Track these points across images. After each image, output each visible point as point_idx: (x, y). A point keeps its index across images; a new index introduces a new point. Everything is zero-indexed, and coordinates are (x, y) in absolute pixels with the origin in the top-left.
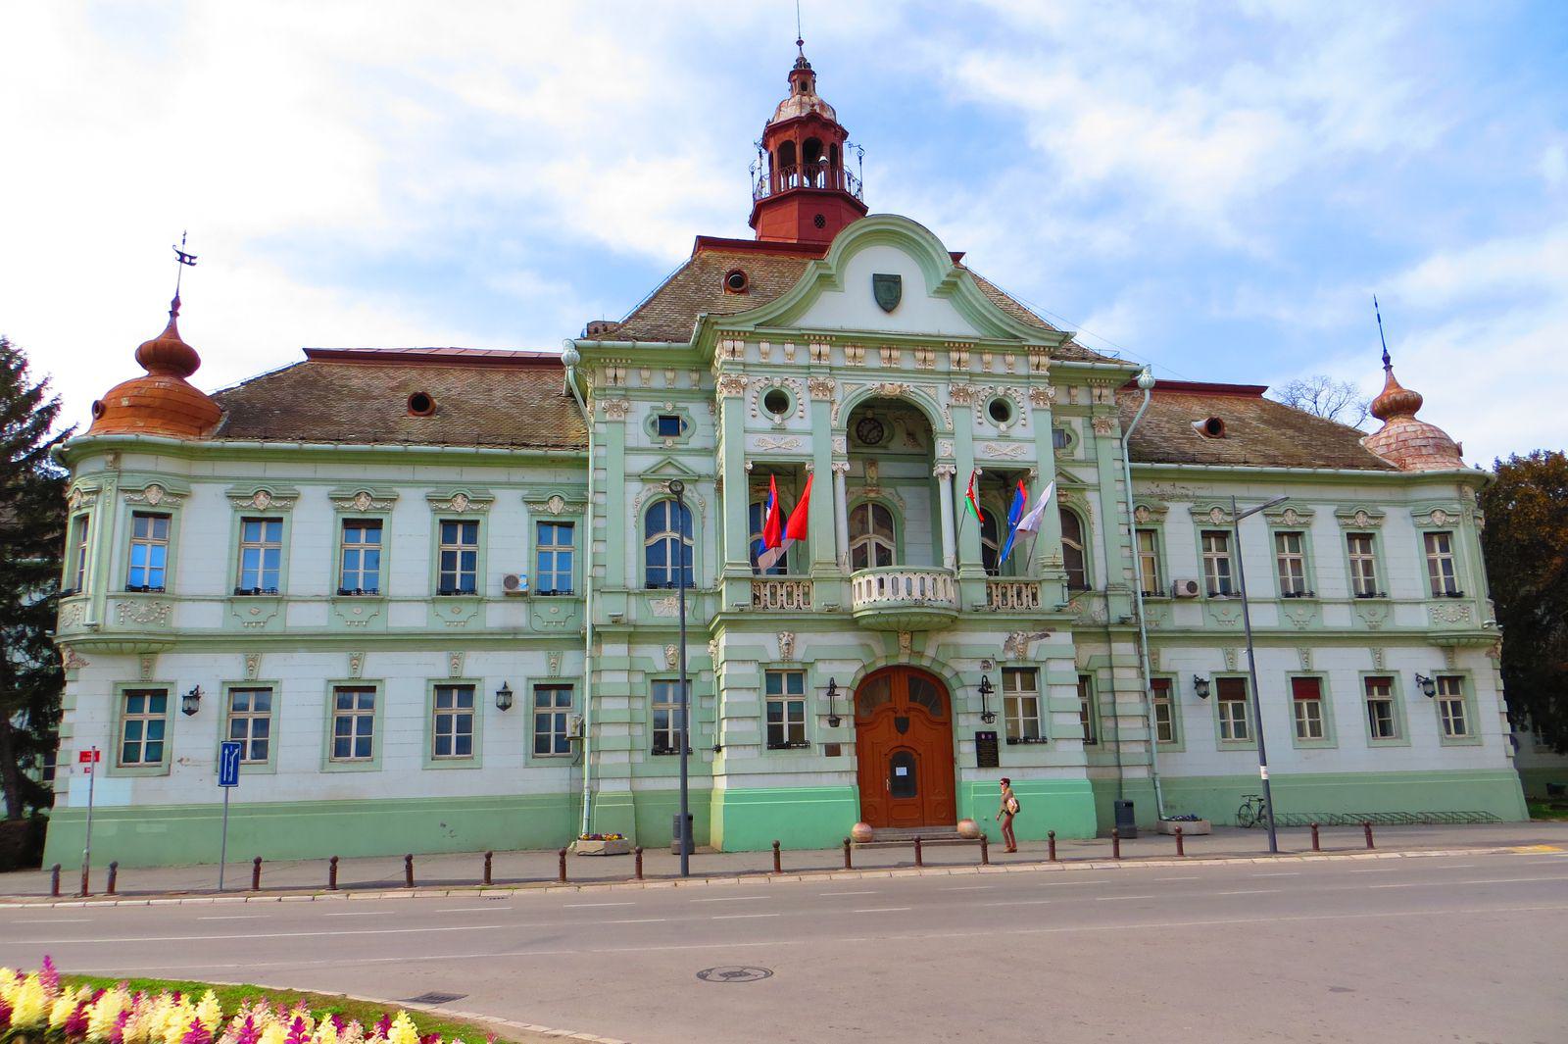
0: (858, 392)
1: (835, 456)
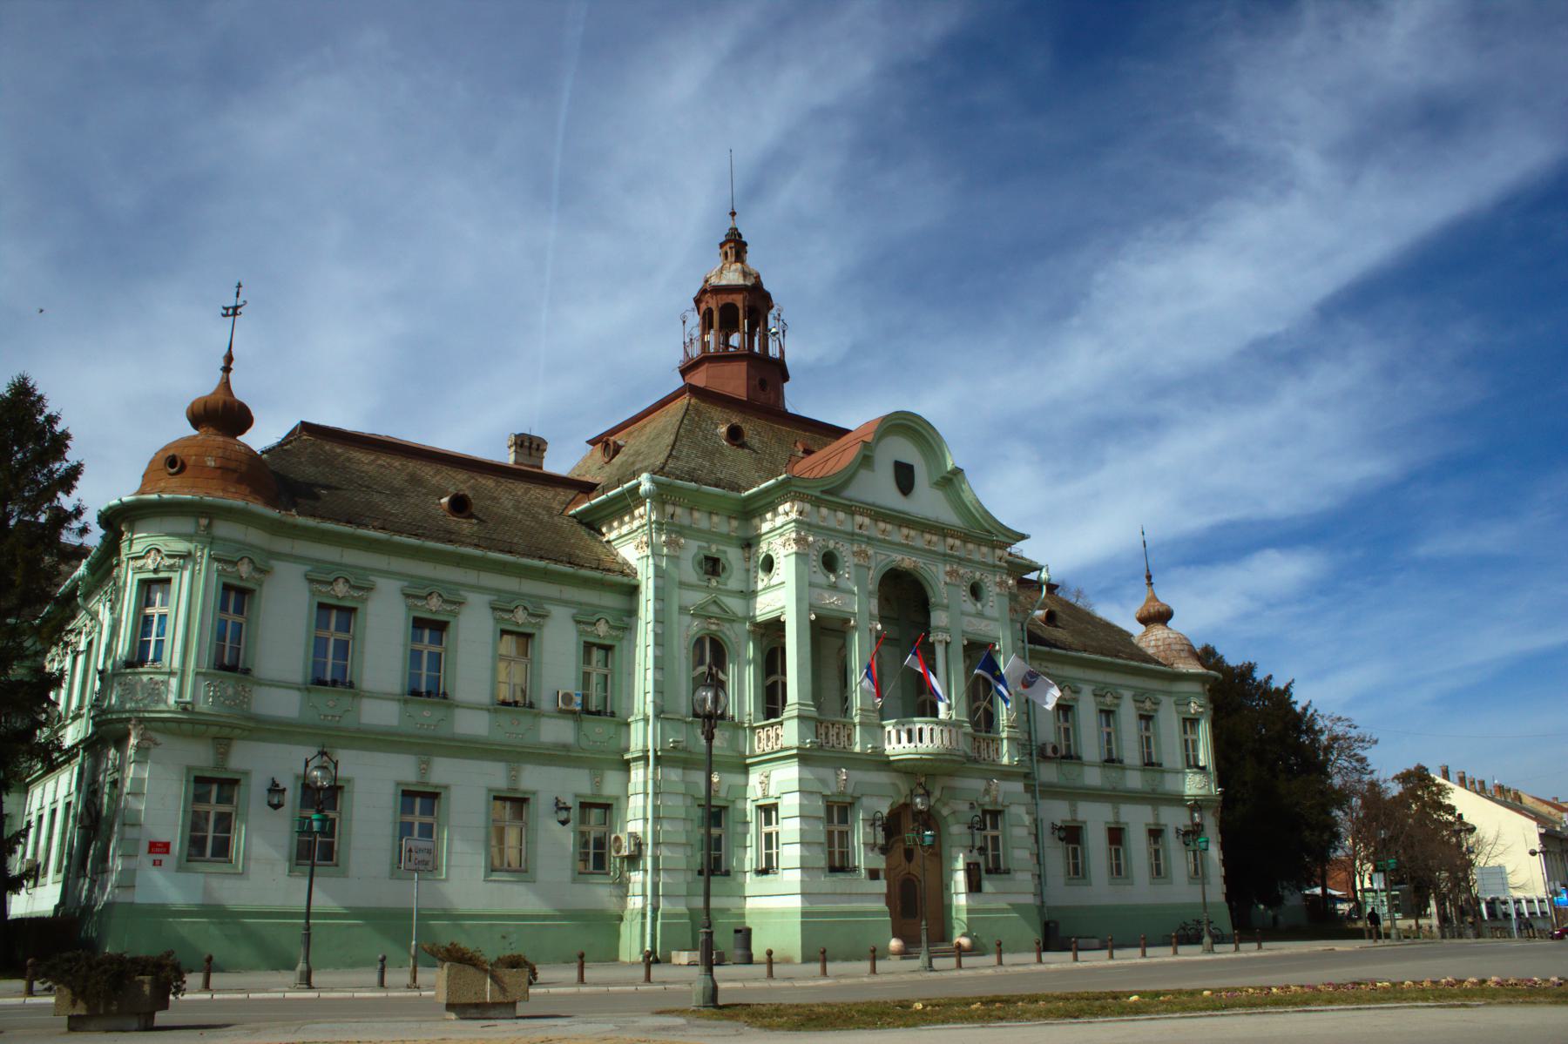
0: (885, 562)
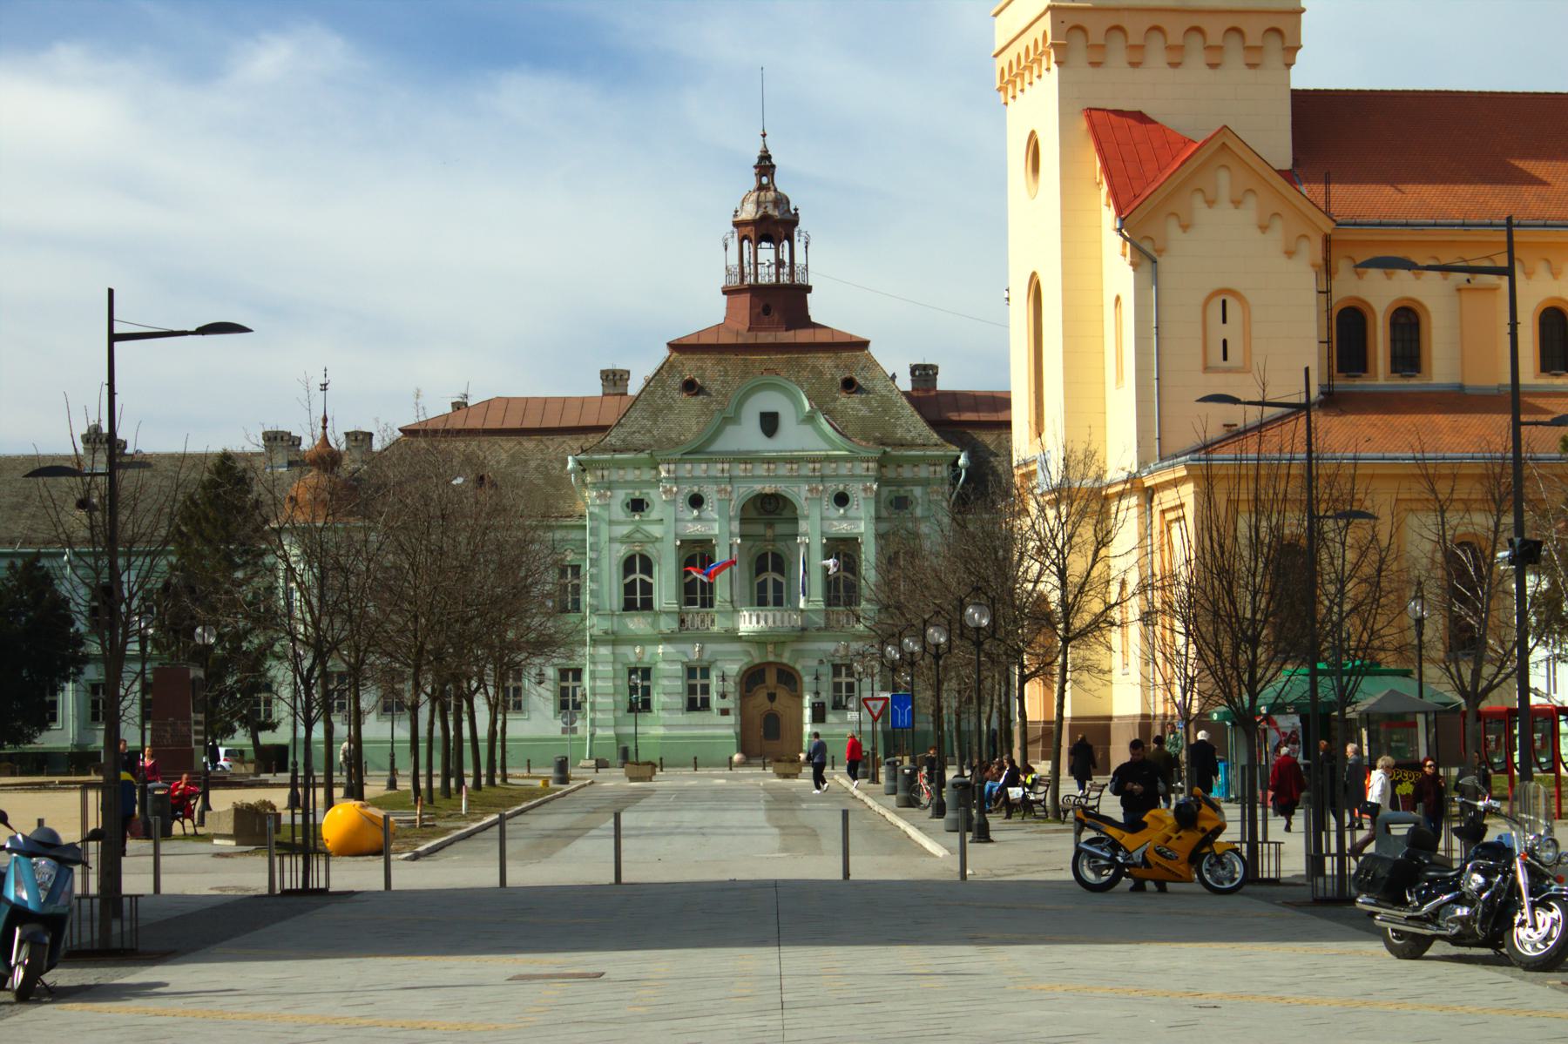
1: (731, 535)
